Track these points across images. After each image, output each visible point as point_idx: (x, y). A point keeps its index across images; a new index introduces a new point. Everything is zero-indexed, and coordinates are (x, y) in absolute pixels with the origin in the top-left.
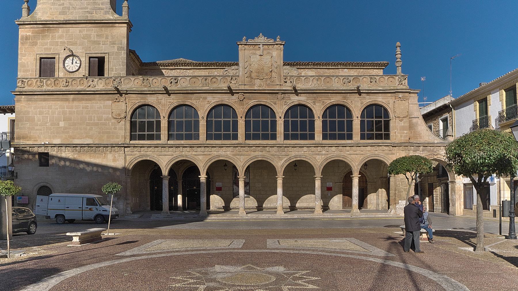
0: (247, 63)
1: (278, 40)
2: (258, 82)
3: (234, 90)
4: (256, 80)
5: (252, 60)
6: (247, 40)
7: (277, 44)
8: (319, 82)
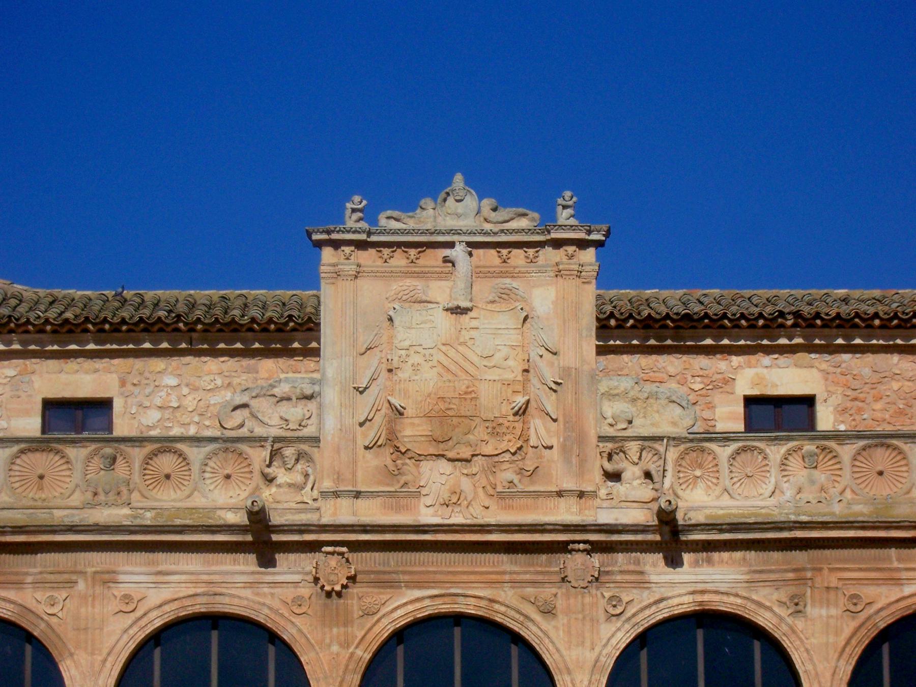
0: (373, 361)
1: (564, 216)
2: (436, 477)
3: (280, 529)
4: (426, 466)
5: (404, 336)
7: (558, 244)
8: (821, 476)
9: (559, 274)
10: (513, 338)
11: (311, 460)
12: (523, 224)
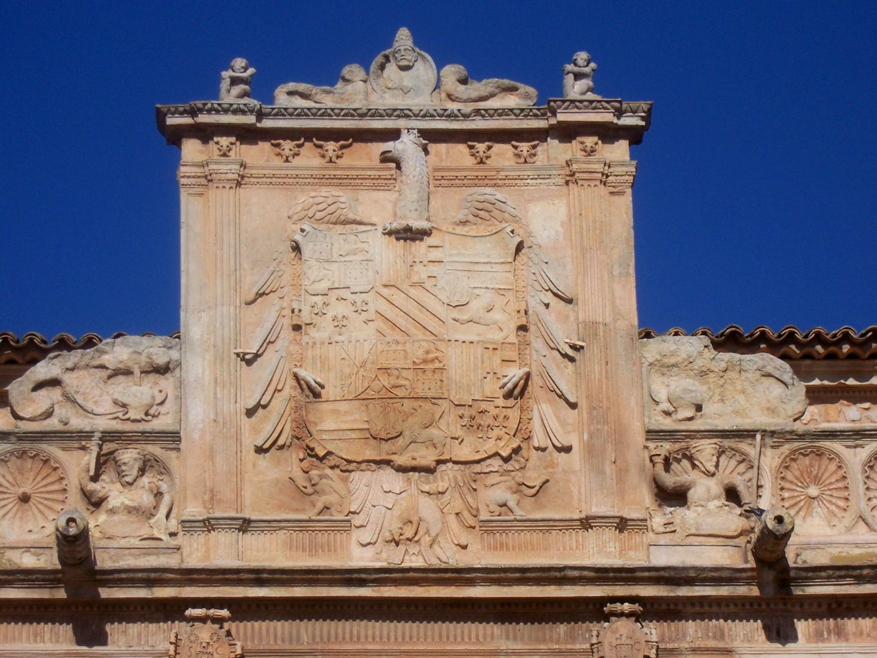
0: (269, 313)
1: (575, 89)
4: (360, 479)
5: (317, 274)
6: (261, 88)
7: (567, 132)
9: (571, 179)
10: (501, 277)
11: (164, 470)
12: (512, 101)
